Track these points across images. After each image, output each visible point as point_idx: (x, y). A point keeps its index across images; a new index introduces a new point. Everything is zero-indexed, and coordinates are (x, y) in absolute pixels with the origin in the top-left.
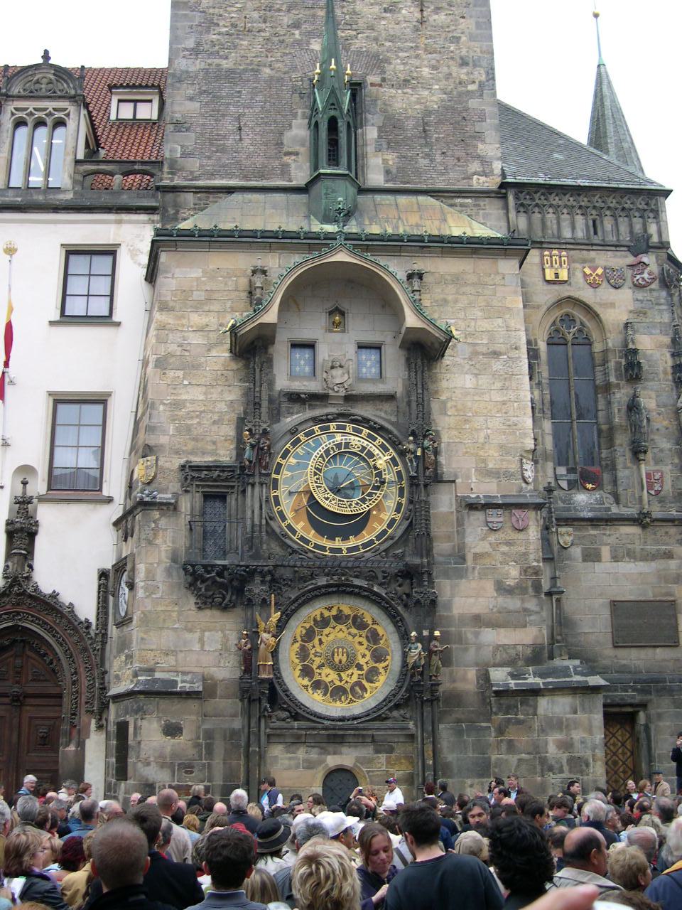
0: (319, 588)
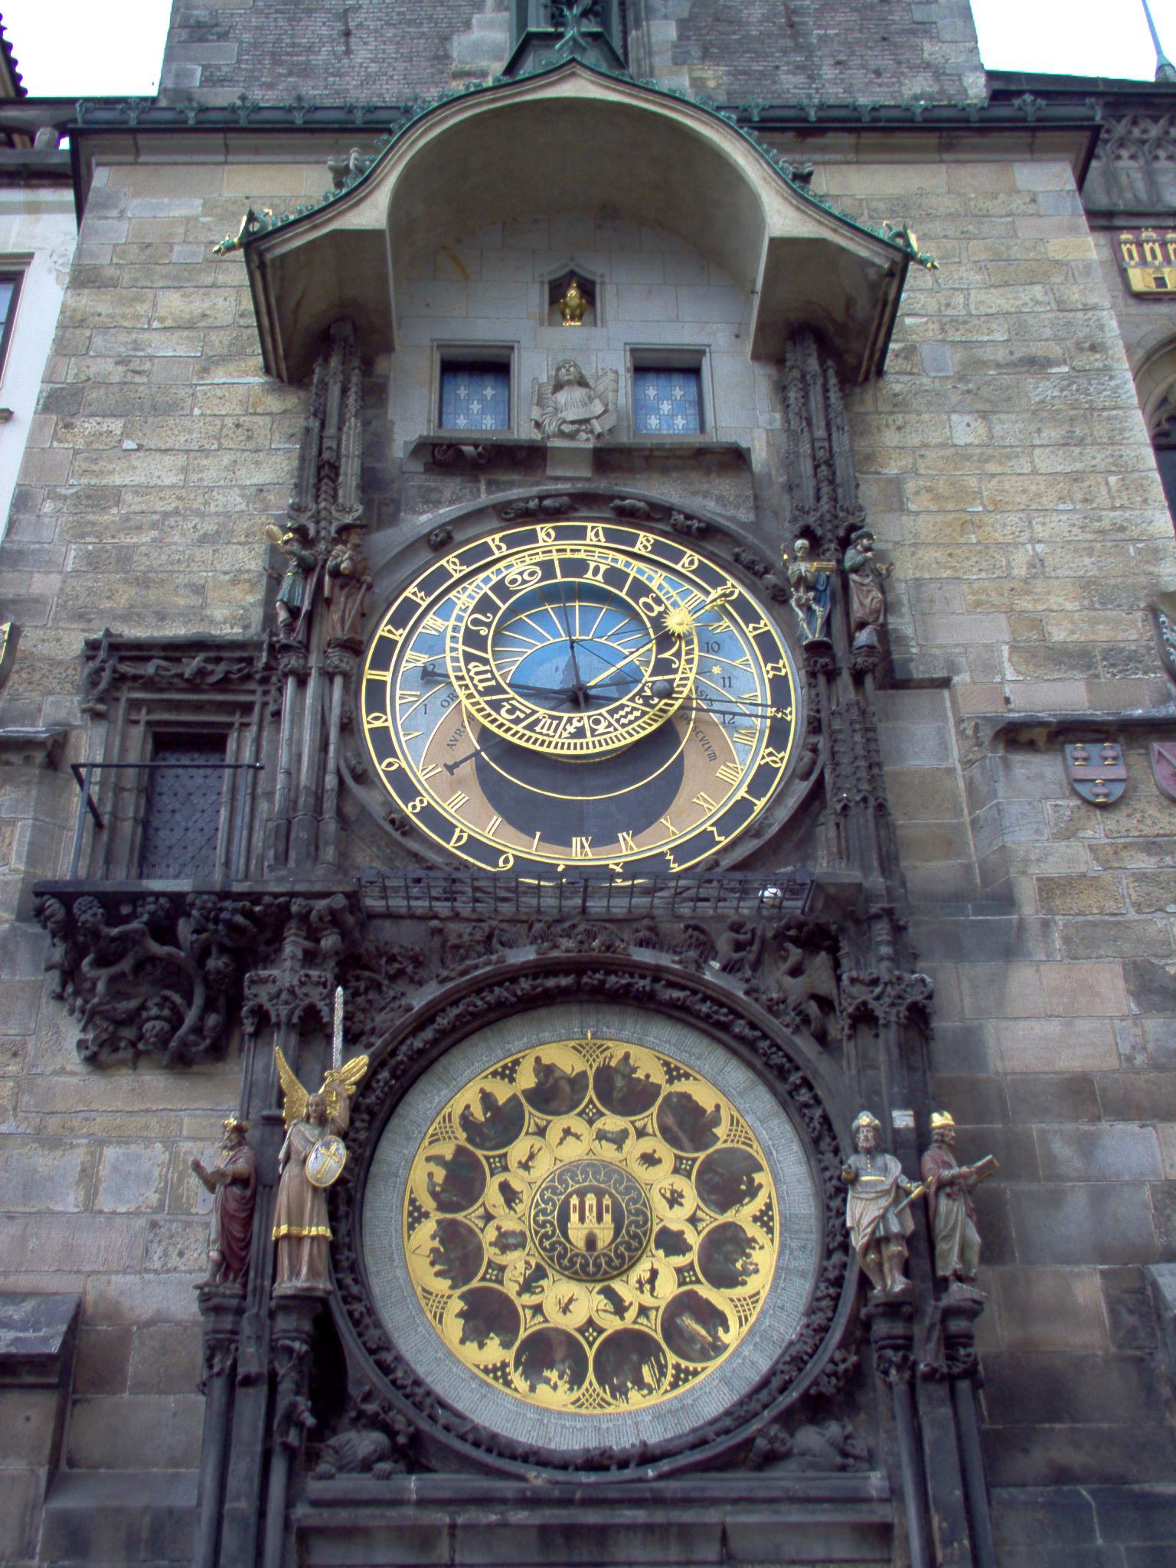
0: (512, 976)
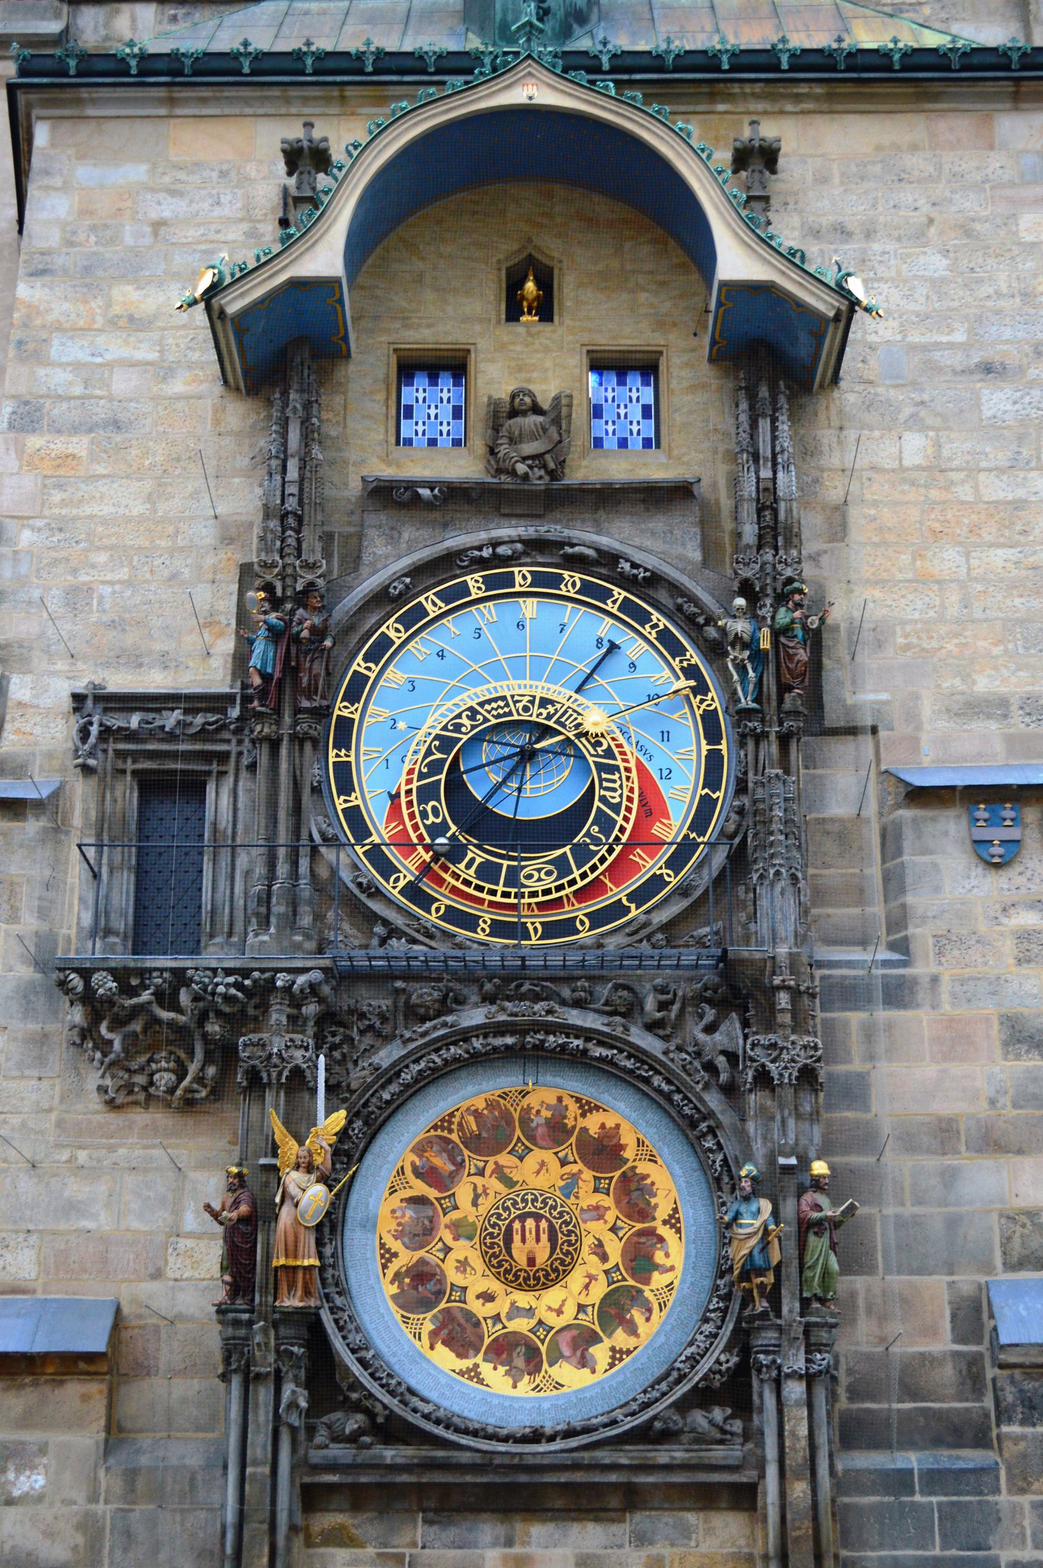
0: (465, 1035)
